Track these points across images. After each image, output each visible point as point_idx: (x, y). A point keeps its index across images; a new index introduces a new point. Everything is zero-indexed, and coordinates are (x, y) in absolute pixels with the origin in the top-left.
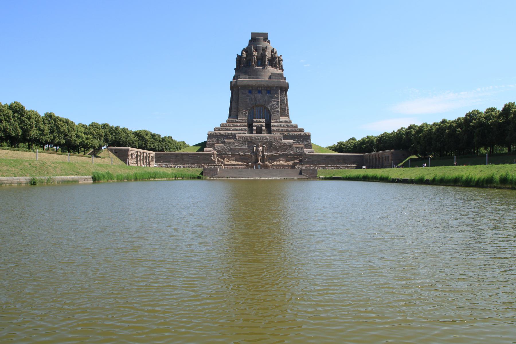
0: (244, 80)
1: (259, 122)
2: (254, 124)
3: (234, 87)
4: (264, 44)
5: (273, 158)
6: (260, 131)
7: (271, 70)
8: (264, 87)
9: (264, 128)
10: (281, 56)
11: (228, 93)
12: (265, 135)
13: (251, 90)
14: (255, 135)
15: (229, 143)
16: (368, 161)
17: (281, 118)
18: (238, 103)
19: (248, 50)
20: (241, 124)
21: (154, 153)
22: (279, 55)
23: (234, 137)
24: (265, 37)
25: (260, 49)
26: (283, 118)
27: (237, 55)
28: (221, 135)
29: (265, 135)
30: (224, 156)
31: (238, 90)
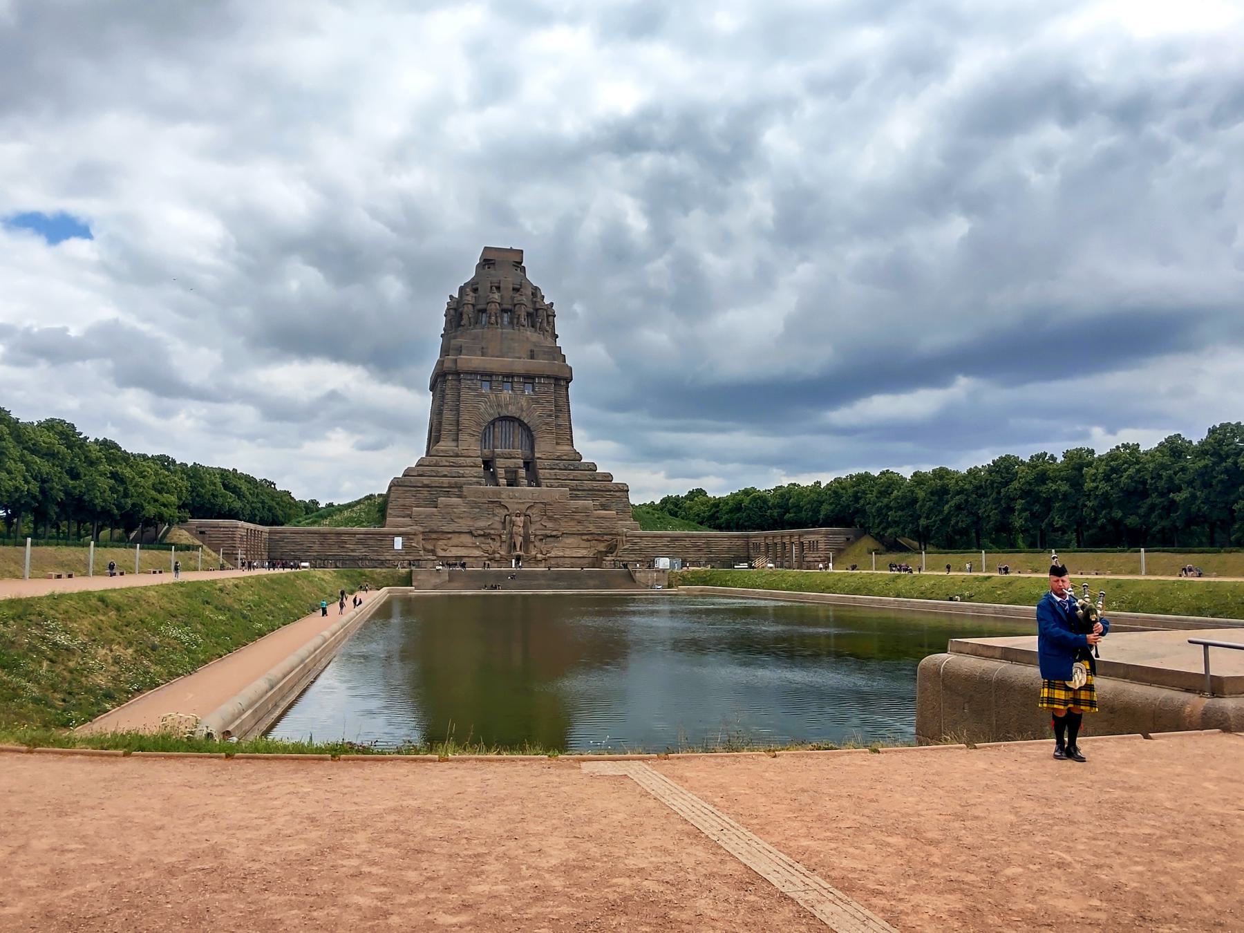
2: (500, 462)
6: (512, 483)
8: (519, 376)
9: (522, 472)
10: (552, 304)
15: (447, 506)
16: (763, 549)
17: (559, 447)
18: (458, 410)
20: (468, 460)
21: (267, 528)
22: (547, 301)
25: (507, 288)
27: (451, 297)
30: (434, 536)
31: (459, 381)
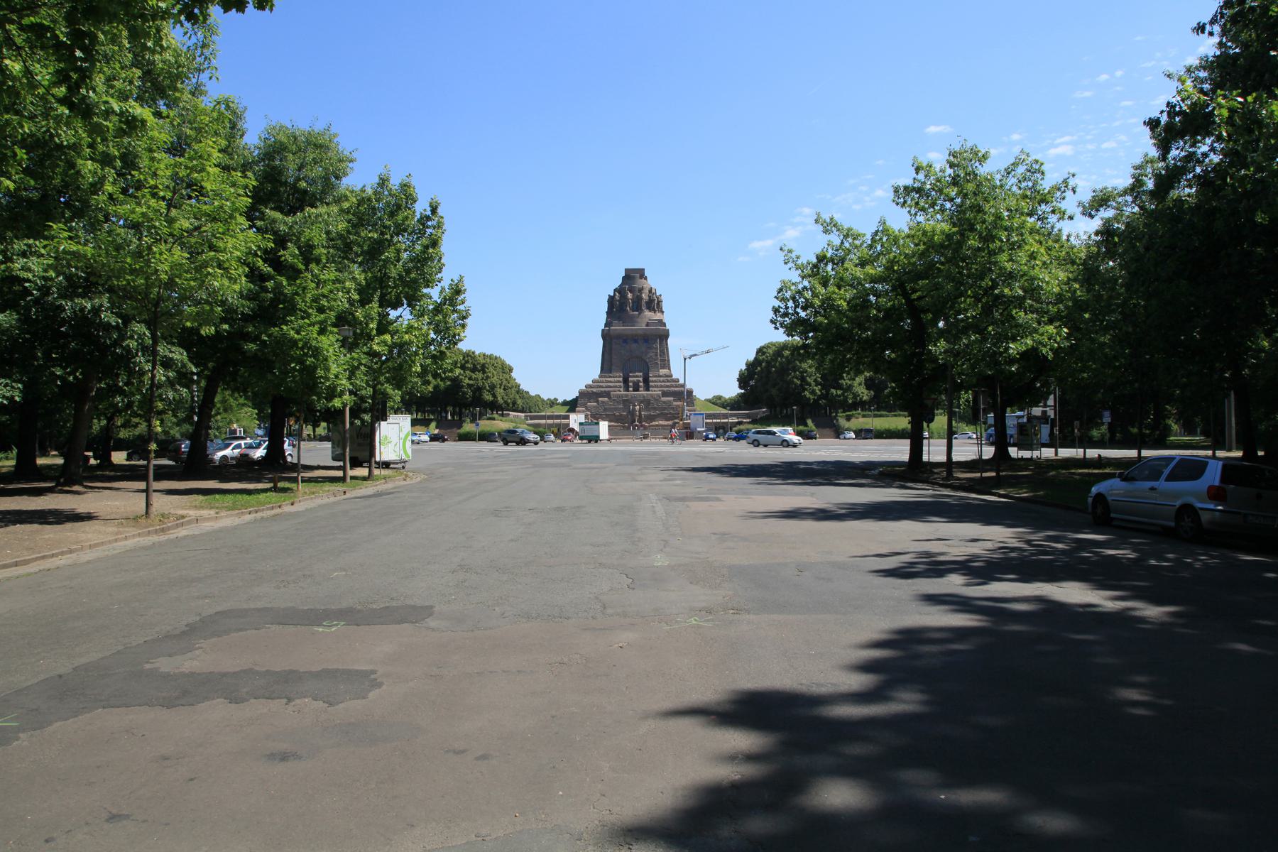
0: (618, 328)
1: (637, 377)
3: (606, 335)
4: (639, 283)
5: (651, 418)
6: (636, 388)
7: (648, 314)
11: (600, 343)
12: (642, 392)
13: (626, 339)
14: (631, 393)
19: (620, 290)
23: (607, 394)
24: (641, 273)
26: (662, 372)
28: (593, 393)
29: (642, 392)
